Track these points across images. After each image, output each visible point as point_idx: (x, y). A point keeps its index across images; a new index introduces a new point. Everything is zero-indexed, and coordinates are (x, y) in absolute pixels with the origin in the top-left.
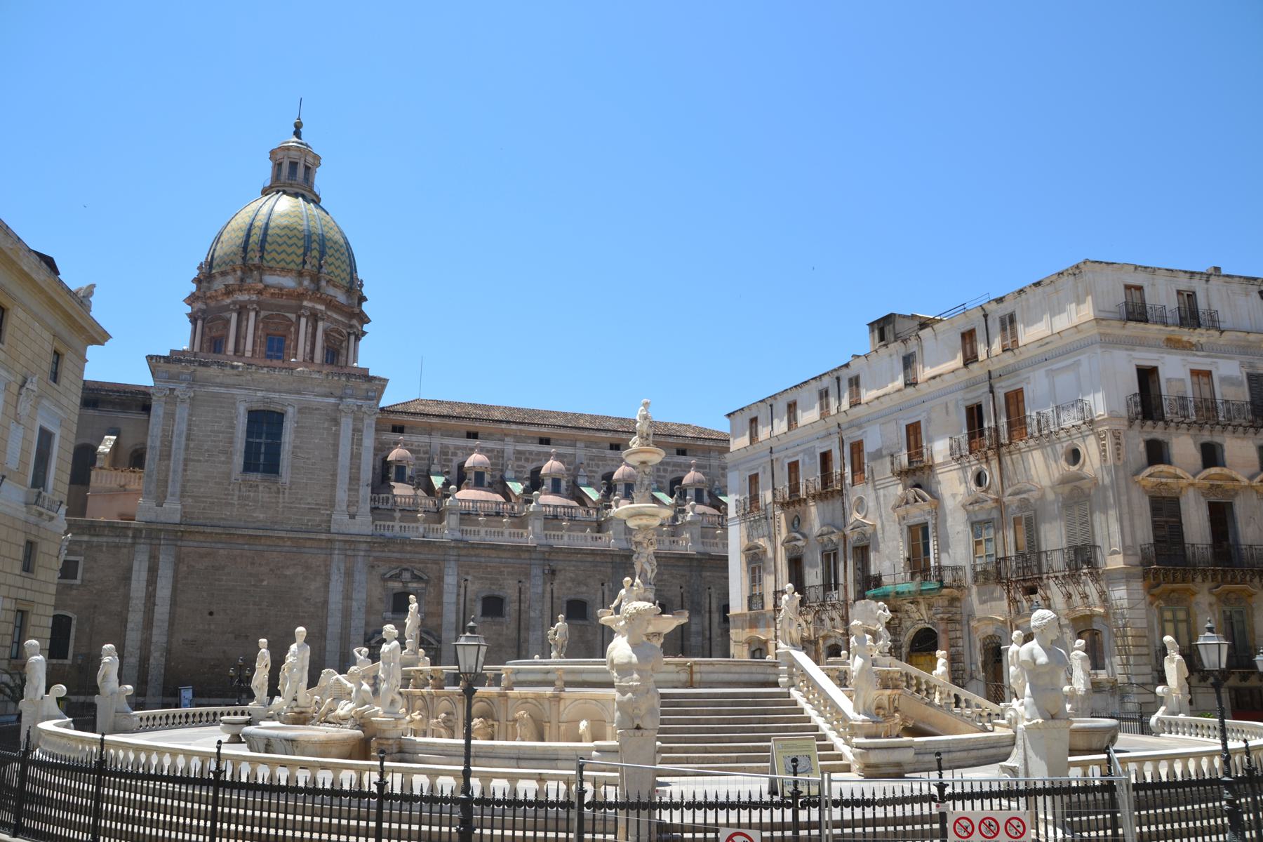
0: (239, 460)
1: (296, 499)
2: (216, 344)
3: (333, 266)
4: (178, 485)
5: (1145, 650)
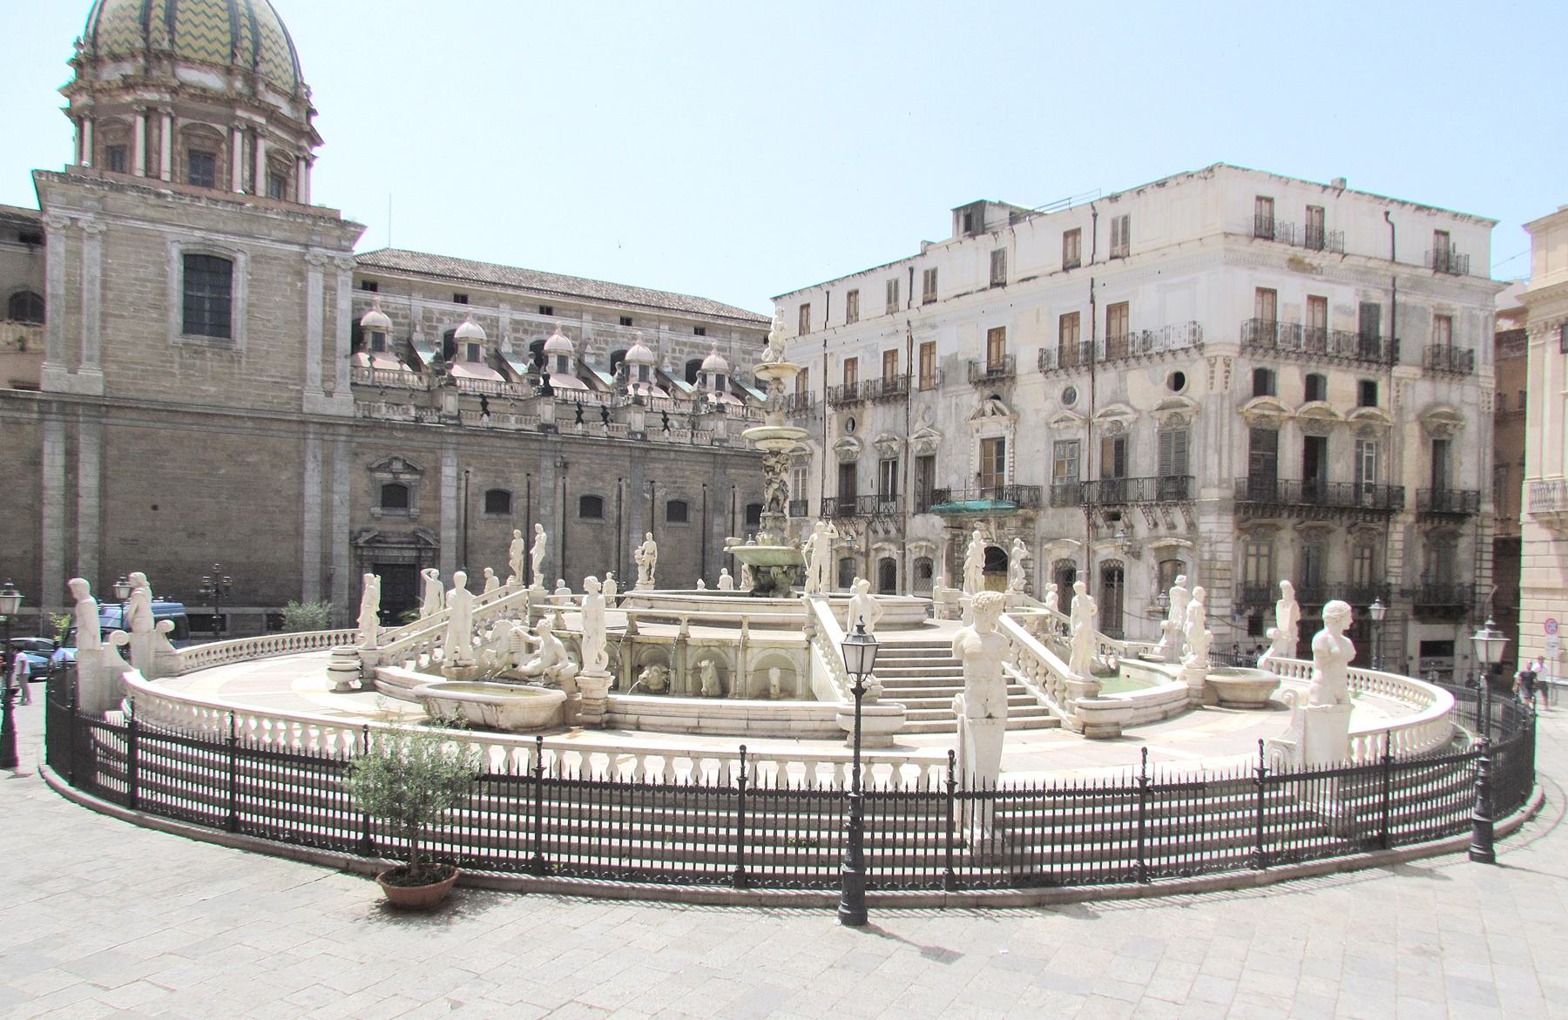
0: (176, 318)
1: (257, 370)
2: (116, 157)
3: (271, 64)
4: (96, 347)
5: (1227, 584)
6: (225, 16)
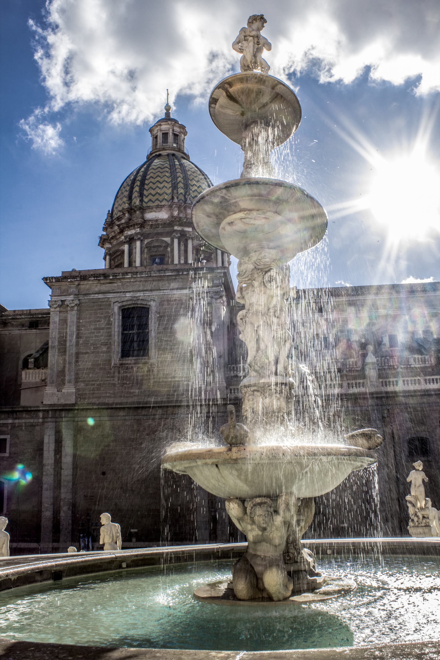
0: (117, 348)
4: (73, 373)
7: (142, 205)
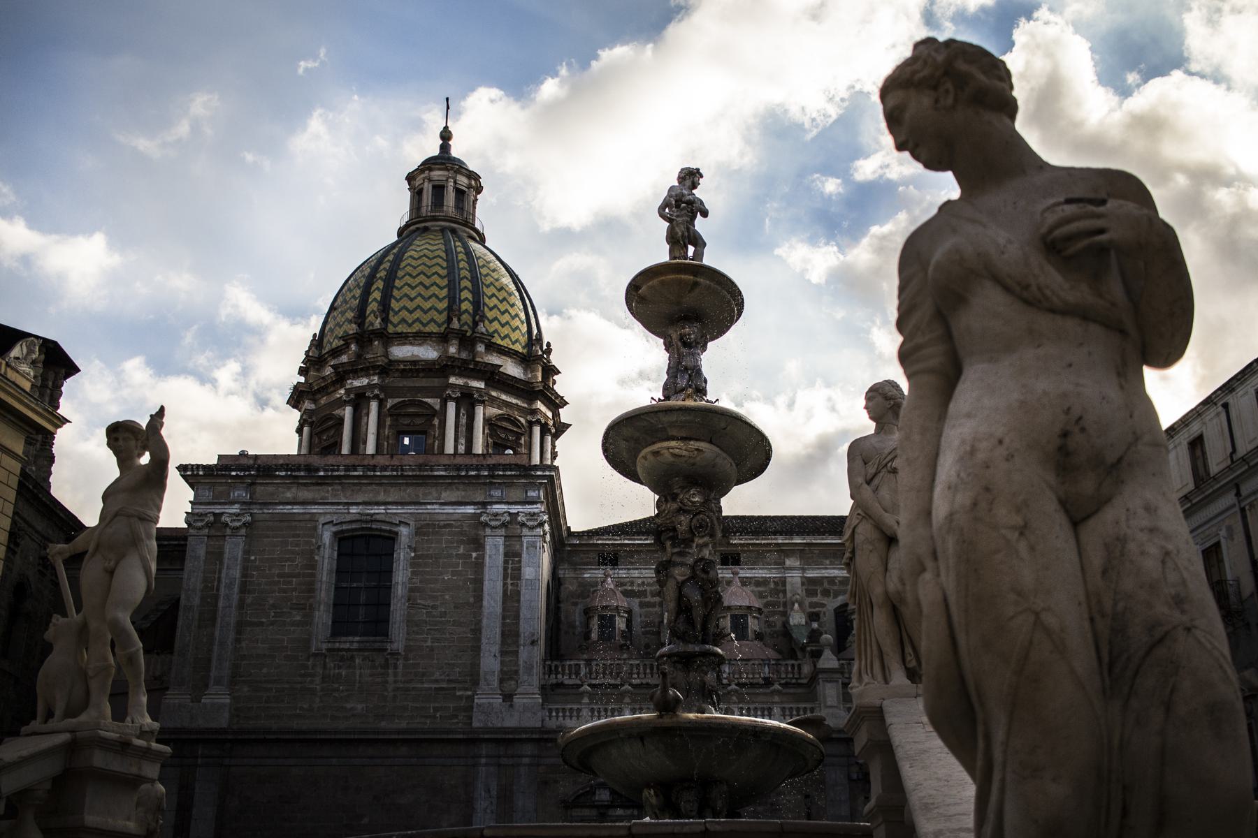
0: (323, 617)
6: (445, 282)
7: (385, 329)
